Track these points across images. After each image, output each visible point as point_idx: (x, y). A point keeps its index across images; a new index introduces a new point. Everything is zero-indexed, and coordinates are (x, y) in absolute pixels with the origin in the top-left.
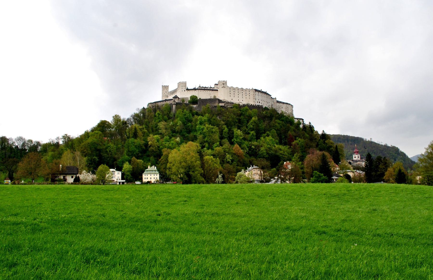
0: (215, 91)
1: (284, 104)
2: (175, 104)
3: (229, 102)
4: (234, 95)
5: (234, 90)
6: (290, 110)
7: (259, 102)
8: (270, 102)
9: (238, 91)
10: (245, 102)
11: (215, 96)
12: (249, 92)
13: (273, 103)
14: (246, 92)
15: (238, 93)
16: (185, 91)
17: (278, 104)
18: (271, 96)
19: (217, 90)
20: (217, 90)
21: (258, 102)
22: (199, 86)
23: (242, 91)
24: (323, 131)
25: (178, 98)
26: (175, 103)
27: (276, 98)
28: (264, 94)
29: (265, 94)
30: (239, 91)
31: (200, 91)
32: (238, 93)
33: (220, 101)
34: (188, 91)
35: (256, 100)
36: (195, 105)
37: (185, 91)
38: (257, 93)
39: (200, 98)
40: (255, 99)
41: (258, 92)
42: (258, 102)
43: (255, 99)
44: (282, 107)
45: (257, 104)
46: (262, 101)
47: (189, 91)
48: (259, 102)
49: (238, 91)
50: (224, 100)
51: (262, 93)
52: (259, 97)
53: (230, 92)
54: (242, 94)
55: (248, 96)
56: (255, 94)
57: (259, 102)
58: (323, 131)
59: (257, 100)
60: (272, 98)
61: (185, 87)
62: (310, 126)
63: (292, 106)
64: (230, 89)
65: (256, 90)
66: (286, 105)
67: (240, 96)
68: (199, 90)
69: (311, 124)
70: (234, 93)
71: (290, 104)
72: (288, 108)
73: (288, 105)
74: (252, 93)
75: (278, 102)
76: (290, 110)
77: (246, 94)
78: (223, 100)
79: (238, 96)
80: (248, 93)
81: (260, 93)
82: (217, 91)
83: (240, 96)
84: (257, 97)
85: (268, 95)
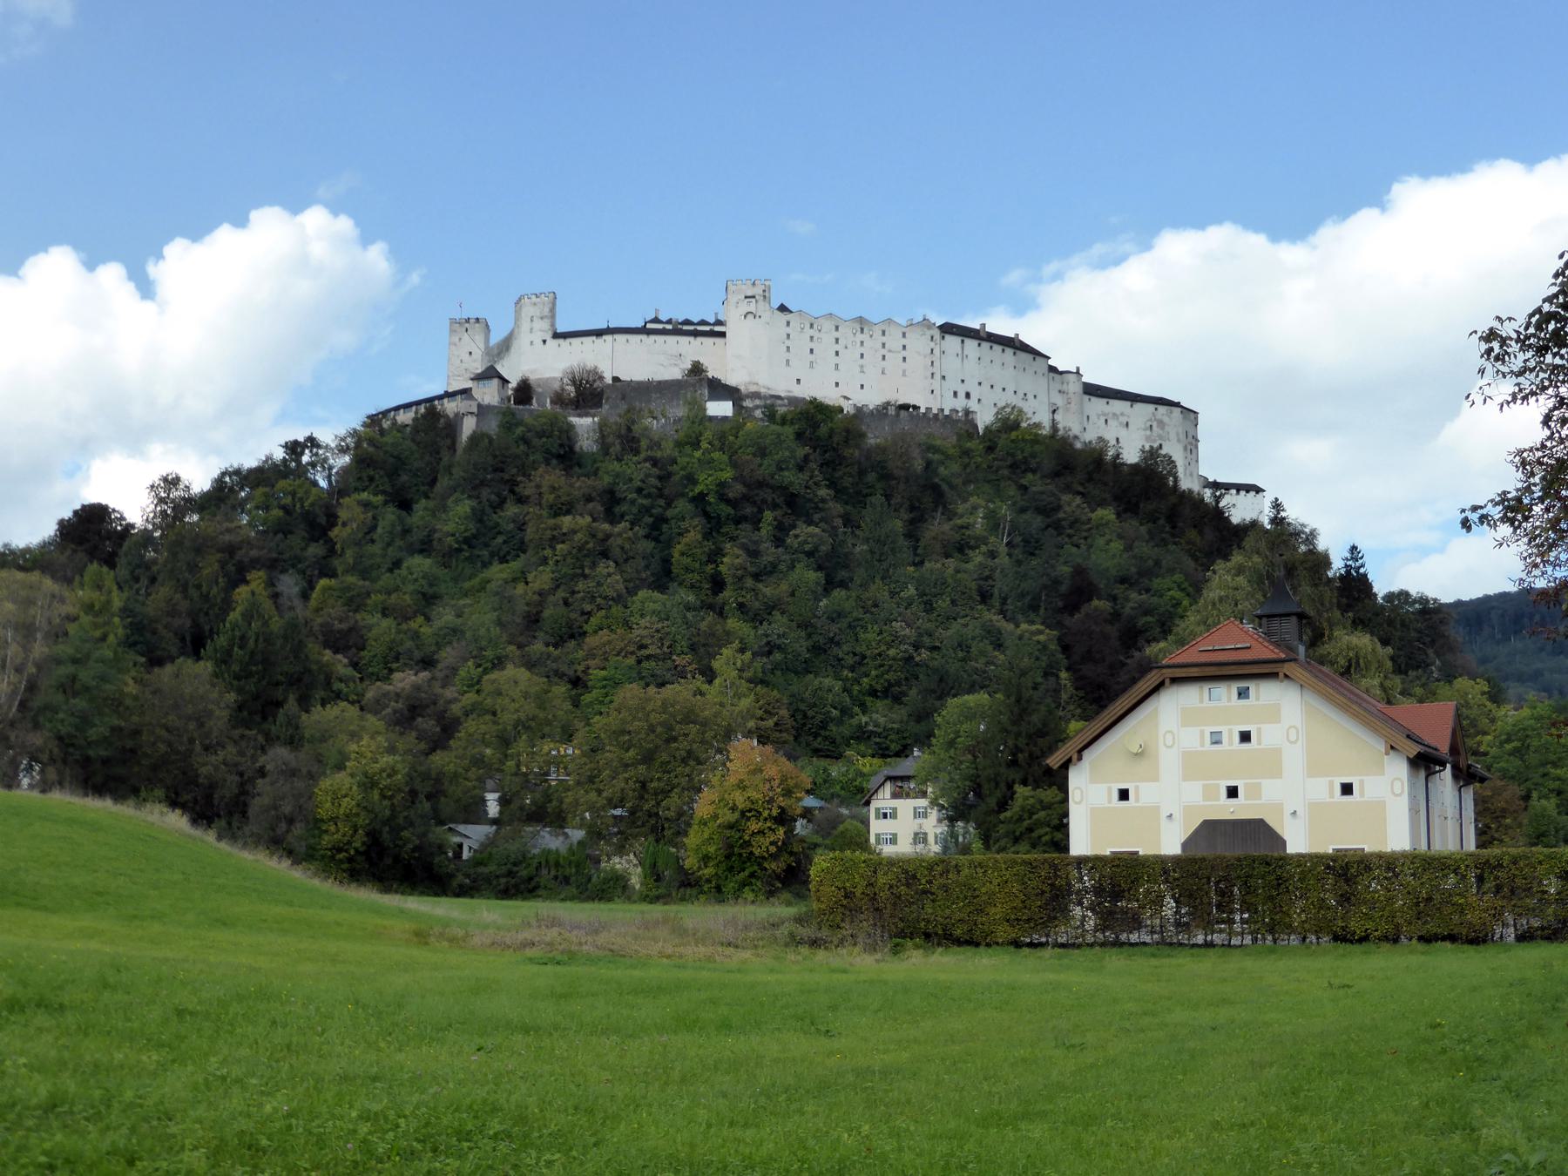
0: (709, 341)
1: (1139, 406)
2: (471, 413)
3: (779, 397)
4: (812, 357)
5: (811, 332)
6: (1173, 436)
7: (968, 395)
8: (1043, 397)
9: (837, 334)
10: (871, 398)
11: (697, 369)
12: (904, 341)
13: (1059, 401)
14: (884, 339)
15: (837, 347)
16: (544, 342)
17: (1098, 405)
18: (1050, 362)
19: (723, 335)
20: (723, 335)
21: (955, 394)
22: (653, 317)
23: (860, 337)
24: (1354, 548)
25: (496, 381)
26: (475, 410)
27: (1078, 372)
28: (997, 348)
29: (1009, 351)
30: (846, 333)
31: (621, 338)
32: (837, 347)
33: (720, 390)
34: (561, 341)
35: (945, 384)
36: (587, 415)
37: (544, 342)
38: (953, 342)
39: (616, 379)
40: (937, 376)
41: (957, 339)
42: (955, 394)
43: (937, 376)
44: (1124, 420)
45: (949, 404)
46: (986, 386)
47: (564, 343)
48: (962, 395)
49: (837, 334)
50: (753, 389)
51: (986, 345)
52: (967, 362)
53: (788, 343)
54: (862, 350)
55: (894, 361)
56: (937, 351)
57: (968, 395)
58: (1354, 548)
59: (952, 384)
60: (1053, 369)
61: (546, 325)
62: (1278, 521)
63: (1195, 412)
64: (788, 323)
65: (948, 329)
66: (1151, 407)
67: (849, 357)
68: (616, 336)
69: (1283, 514)
70: (812, 345)
71: (1177, 405)
72: (1161, 424)
73: (1162, 409)
74: (919, 343)
75: (1093, 391)
76: (1173, 436)
77: (884, 352)
78: (742, 388)
79: (837, 361)
80: (894, 341)
81: (971, 344)
82: (718, 340)
83: (849, 357)
84: (951, 365)
85: (1031, 356)
